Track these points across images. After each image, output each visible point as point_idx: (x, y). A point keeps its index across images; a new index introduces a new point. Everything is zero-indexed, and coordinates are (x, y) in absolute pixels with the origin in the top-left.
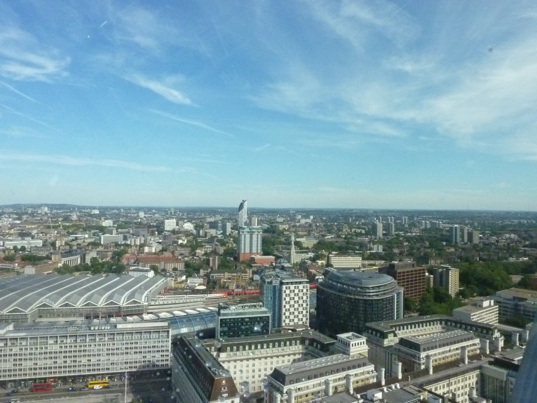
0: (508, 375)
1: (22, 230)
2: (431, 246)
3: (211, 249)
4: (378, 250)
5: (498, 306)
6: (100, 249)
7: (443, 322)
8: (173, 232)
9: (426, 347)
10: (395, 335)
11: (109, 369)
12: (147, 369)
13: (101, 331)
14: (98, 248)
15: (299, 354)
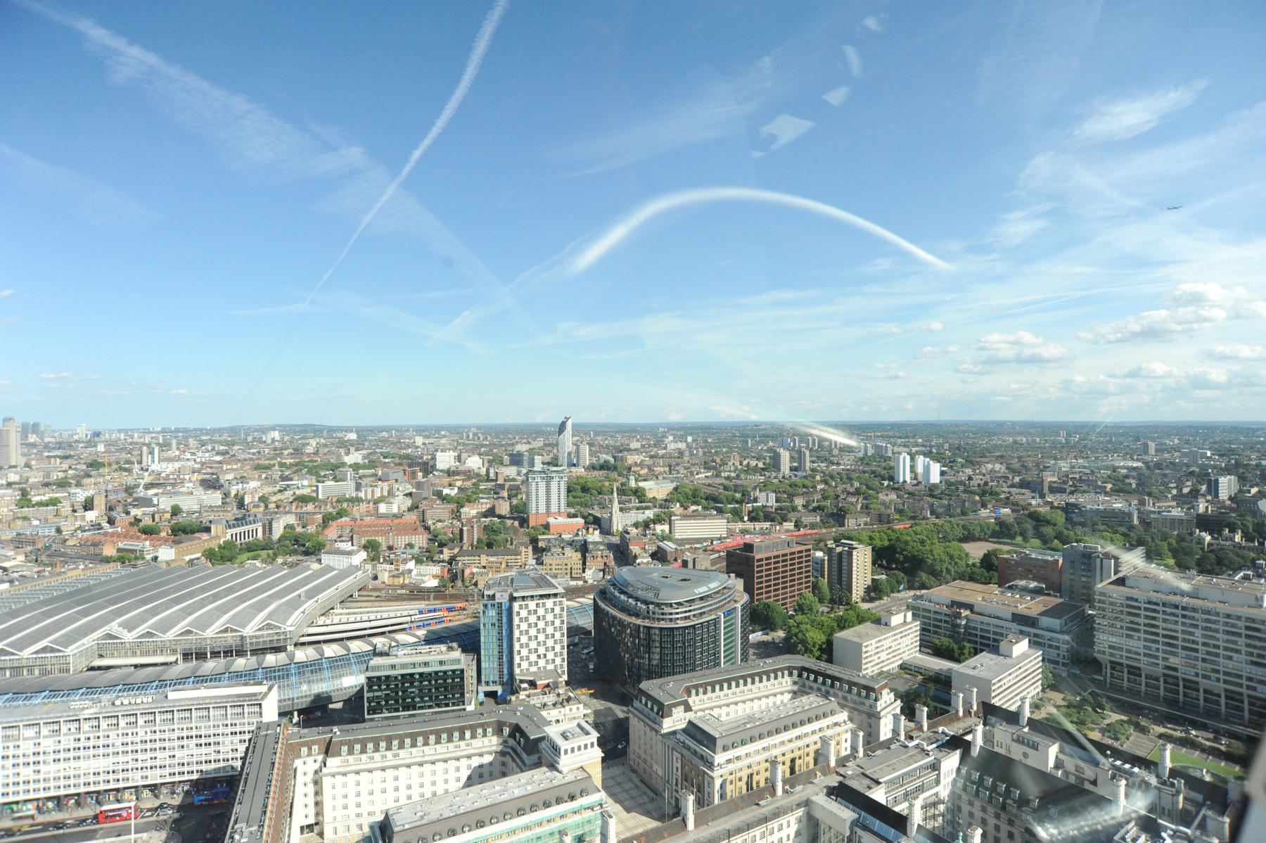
0: (855, 823)
1: (213, 474)
2: (857, 492)
3: (488, 506)
4: (767, 501)
5: (919, 623)
6: (310, 507)
7: (795, 673)
8: (449, 473)
9: (728, 742)
10: (688, 708)
11: (147, 777)
12: (222, 774)
13: (129, 708)
14: (306, 506)
15: (490, 753)
